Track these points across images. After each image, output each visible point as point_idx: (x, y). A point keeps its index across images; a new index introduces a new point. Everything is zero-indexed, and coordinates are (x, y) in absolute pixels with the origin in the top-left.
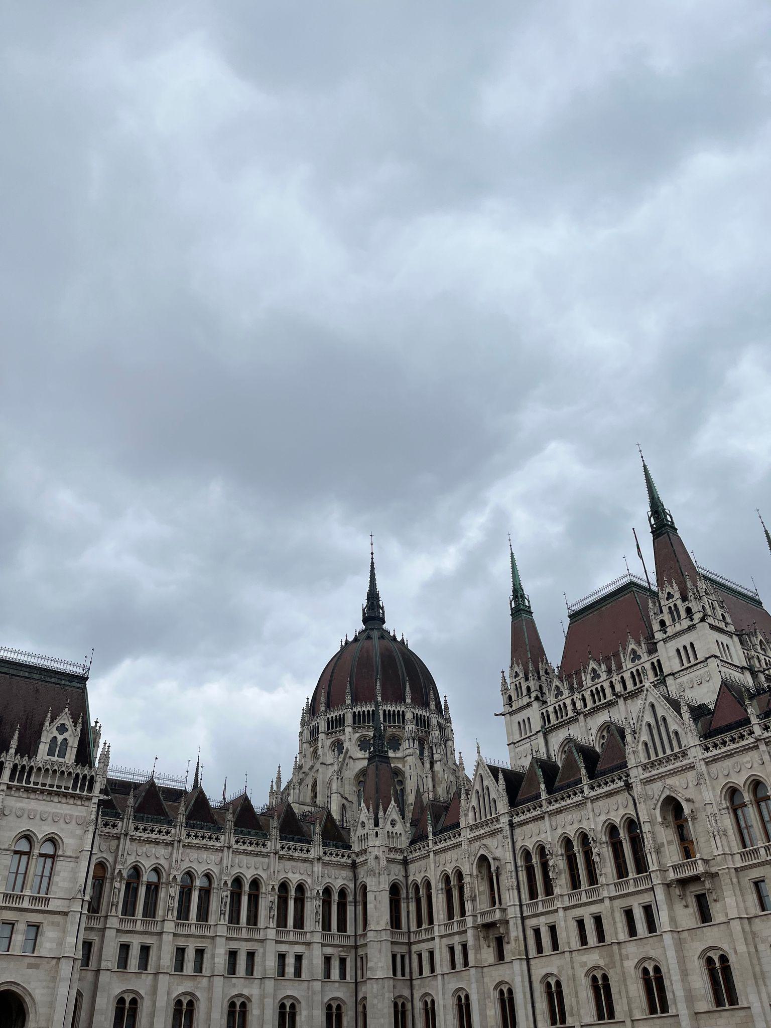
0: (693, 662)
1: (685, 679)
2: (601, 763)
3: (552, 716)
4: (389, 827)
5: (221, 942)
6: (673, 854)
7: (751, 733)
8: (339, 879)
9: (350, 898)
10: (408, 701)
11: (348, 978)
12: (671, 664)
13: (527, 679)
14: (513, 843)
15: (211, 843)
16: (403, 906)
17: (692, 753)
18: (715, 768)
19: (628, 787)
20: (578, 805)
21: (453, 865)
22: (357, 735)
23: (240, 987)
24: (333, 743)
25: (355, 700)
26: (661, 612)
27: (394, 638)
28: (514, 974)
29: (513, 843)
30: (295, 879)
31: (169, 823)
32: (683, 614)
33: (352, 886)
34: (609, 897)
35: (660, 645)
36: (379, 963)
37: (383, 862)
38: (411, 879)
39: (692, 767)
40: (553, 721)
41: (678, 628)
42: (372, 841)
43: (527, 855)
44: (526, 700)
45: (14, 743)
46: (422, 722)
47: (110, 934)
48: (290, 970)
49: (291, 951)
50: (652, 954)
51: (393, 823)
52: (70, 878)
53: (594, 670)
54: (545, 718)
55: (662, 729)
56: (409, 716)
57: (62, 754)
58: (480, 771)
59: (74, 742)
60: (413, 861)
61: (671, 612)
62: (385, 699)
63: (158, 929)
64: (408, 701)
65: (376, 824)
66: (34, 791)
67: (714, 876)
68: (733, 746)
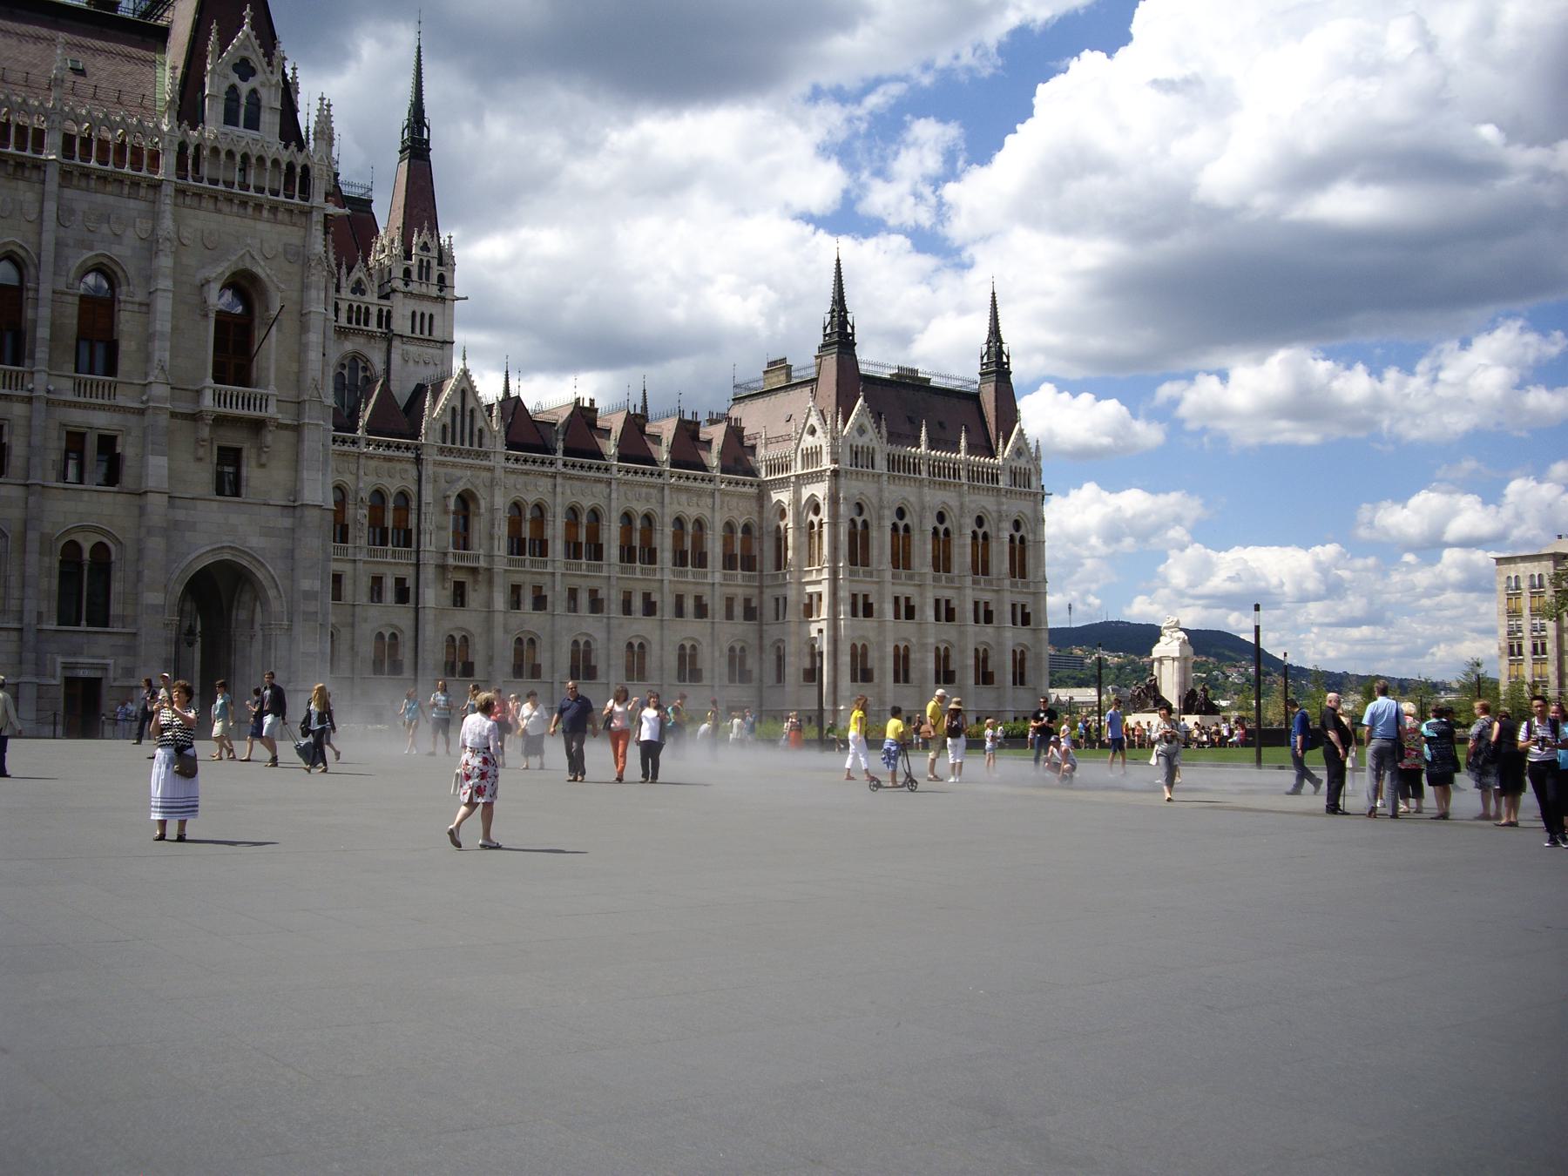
41: (424, 289)
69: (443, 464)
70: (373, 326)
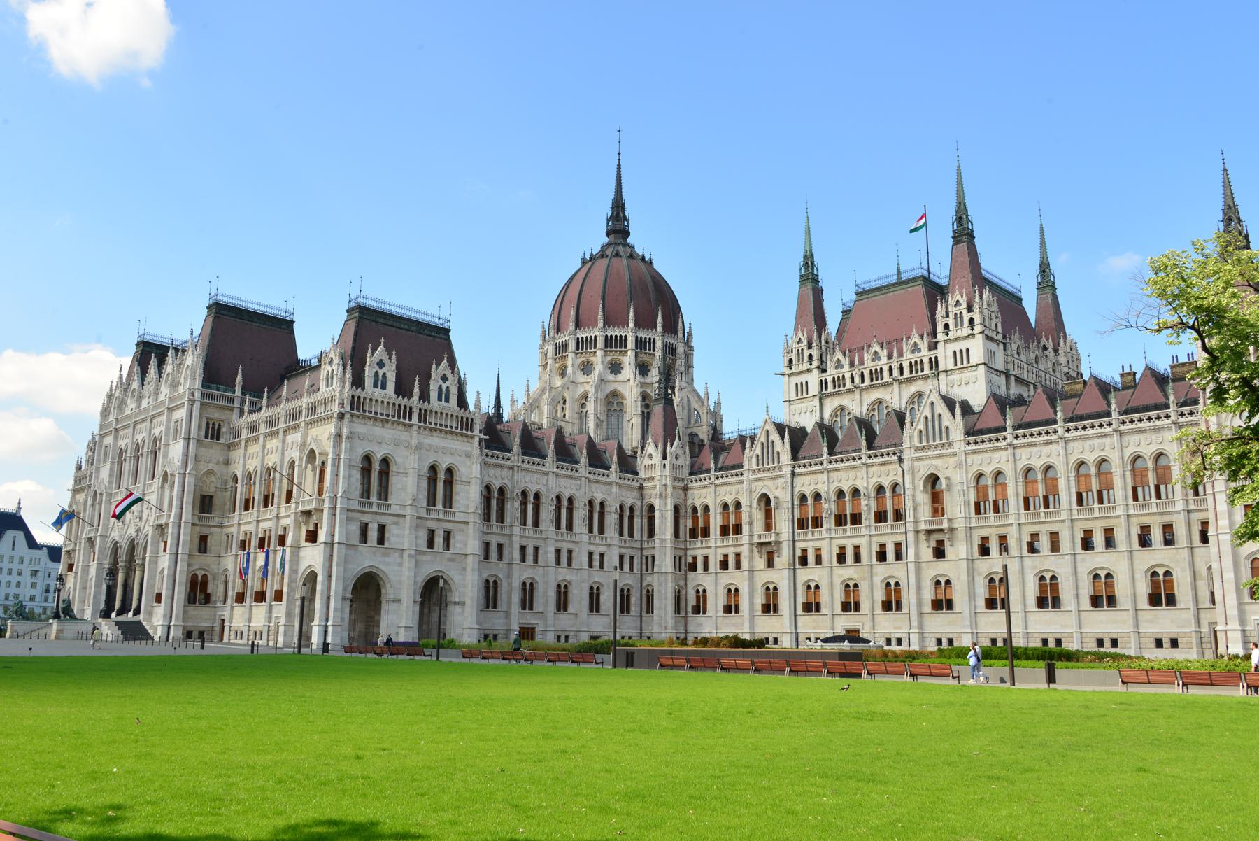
0: (965, 364)
1: (955, 377)
2: (873, 435)
3: (830, 385)
5: (551, 542)
6: (925, 511)
7: (1005, 439)
8: (630, 499)
9: (637, 513)
10: (660, 329)
11: (635, 571)
12: (946, 362)
13: (810, 347)
14: (793, 487)
15: (539, 468)
16: (682, 521)
17: (956, 446)
18: (970, 459)
19: (901, 460)
20: (855, 468)
21: (733, 496)
22: (609, 358)
23: (564, 574)
24: (583, 363)
25: (607, 323)
26: (947, 316)
27: (643, 259)
28: (780, 577)
29: (793, 487)
30: (599, 497)
31: (509, 451)
32: (966, 322)
33: (639, 503)
34: (867, 536)
35: (940, 345)
36: (665, 563)
37: (669, 490)
38: (689, 502)
39: (954, 455)
40: (830, 389)
41: (959, 334)
42: (658, 472)
43: (803, 498)
44: (806, 366)
46: (669, 350)
48: (596, 563)
49: (565, 547)
50: (896, 574)
52: (468, 498)
53: (876, 352)
54: (823, 385)
55: (937, 423)
56: (659, 344)
58: (767, 427)
59: (454, 391)
60: (693, 489)
61: (955, 318)
63: (508, 532)
65: (664, 458)
66: (436, 430)
67: (952, 530)
68: (989, 445)
69: (920, 459)
70: (927, 370)
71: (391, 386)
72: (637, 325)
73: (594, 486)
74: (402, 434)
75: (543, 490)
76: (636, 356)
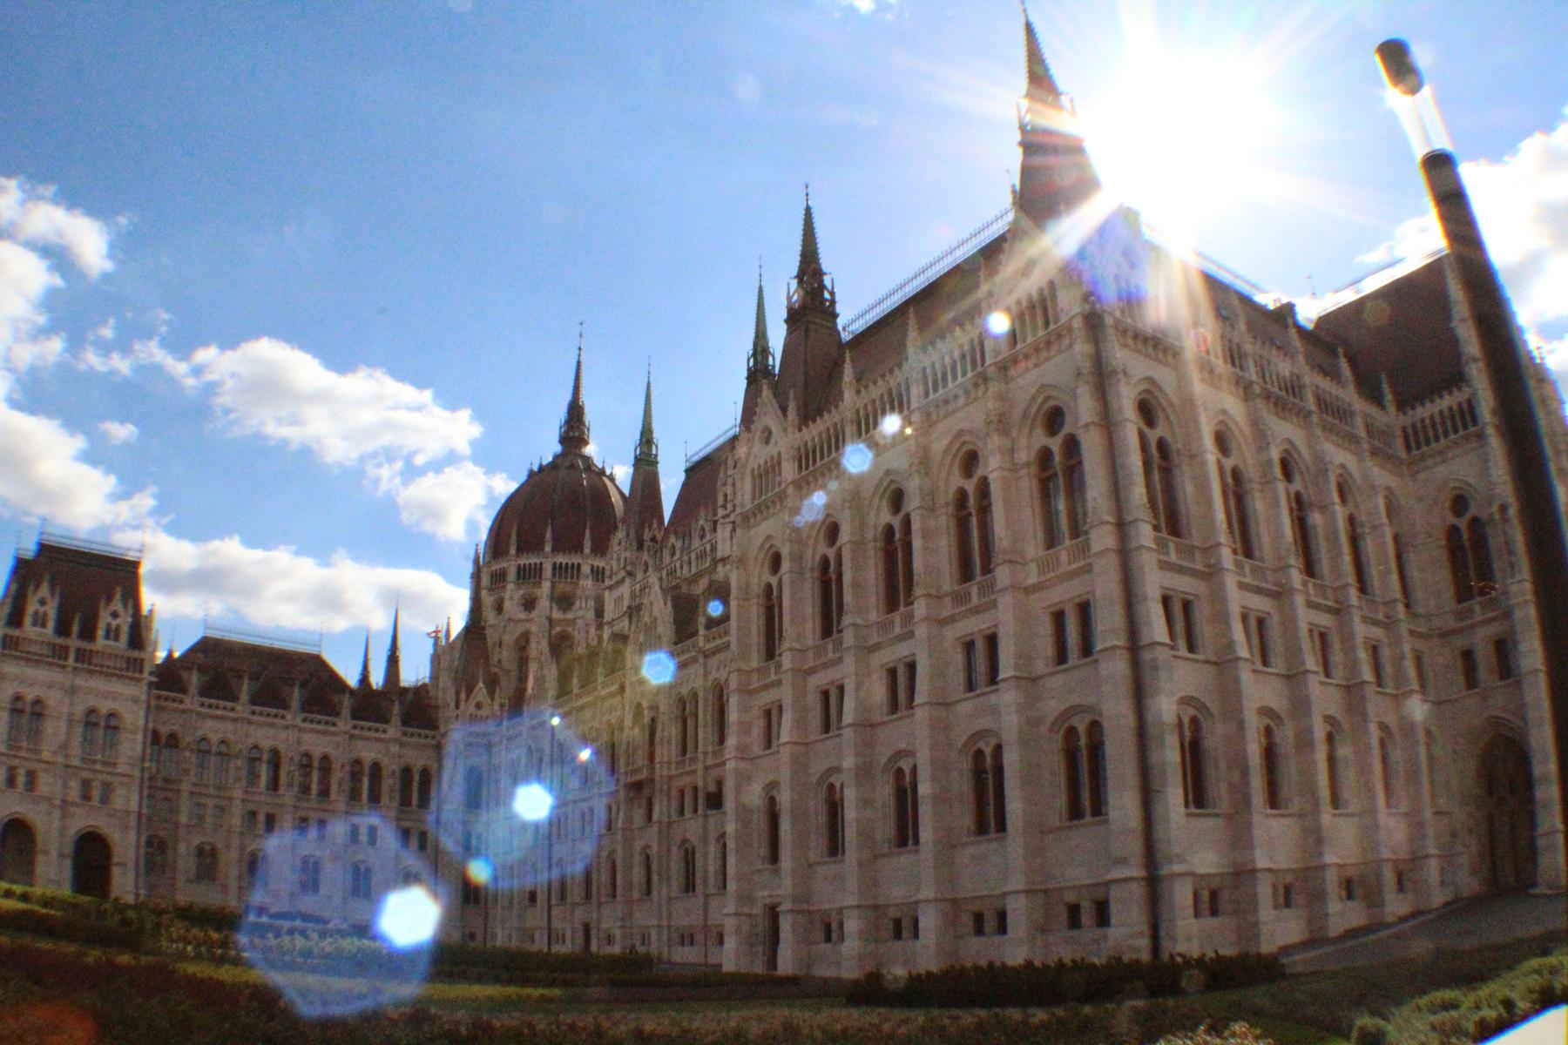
4: (472, 709)
10: (587, 550)
45: (75, 629)
47: (185, 795)
51: (479, 706)
52: (131, 745)
56: (586, 569)
57: (117, 639)
59: (125, 629)
62: (556, 548)
64: (587, 550)
65: (457, 707)
71: (51, 624)
72: (556, 548)
73: (360, 744)
74: (56, 676)
75: (282, 747)
76: (553, 585)
